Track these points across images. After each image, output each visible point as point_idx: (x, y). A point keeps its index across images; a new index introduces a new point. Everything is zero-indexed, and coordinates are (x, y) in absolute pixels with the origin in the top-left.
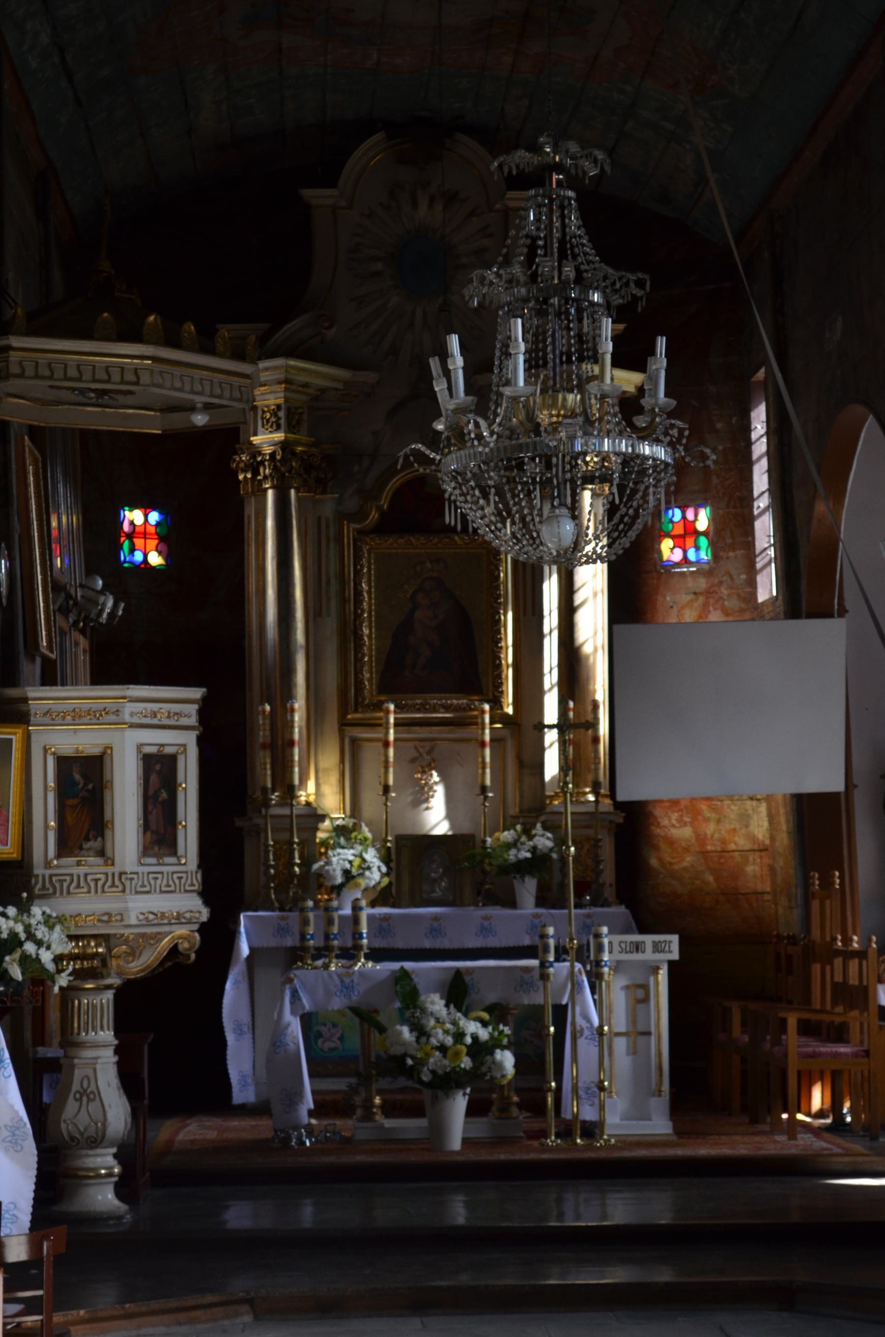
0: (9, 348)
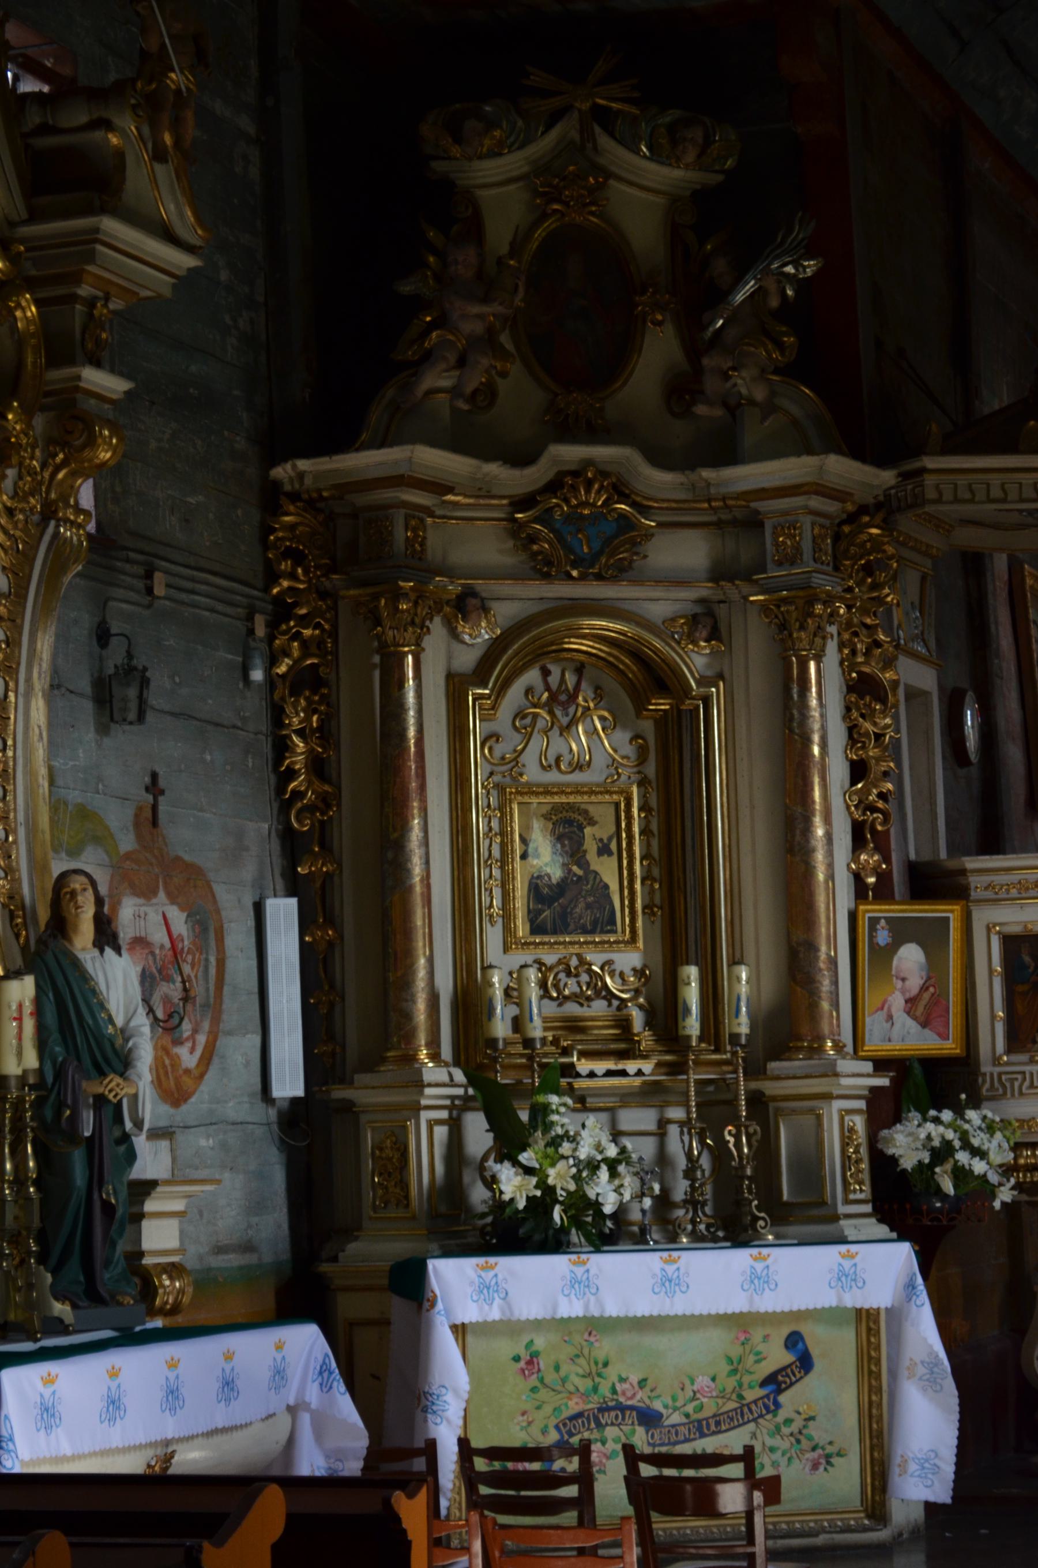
0: (924, 470)
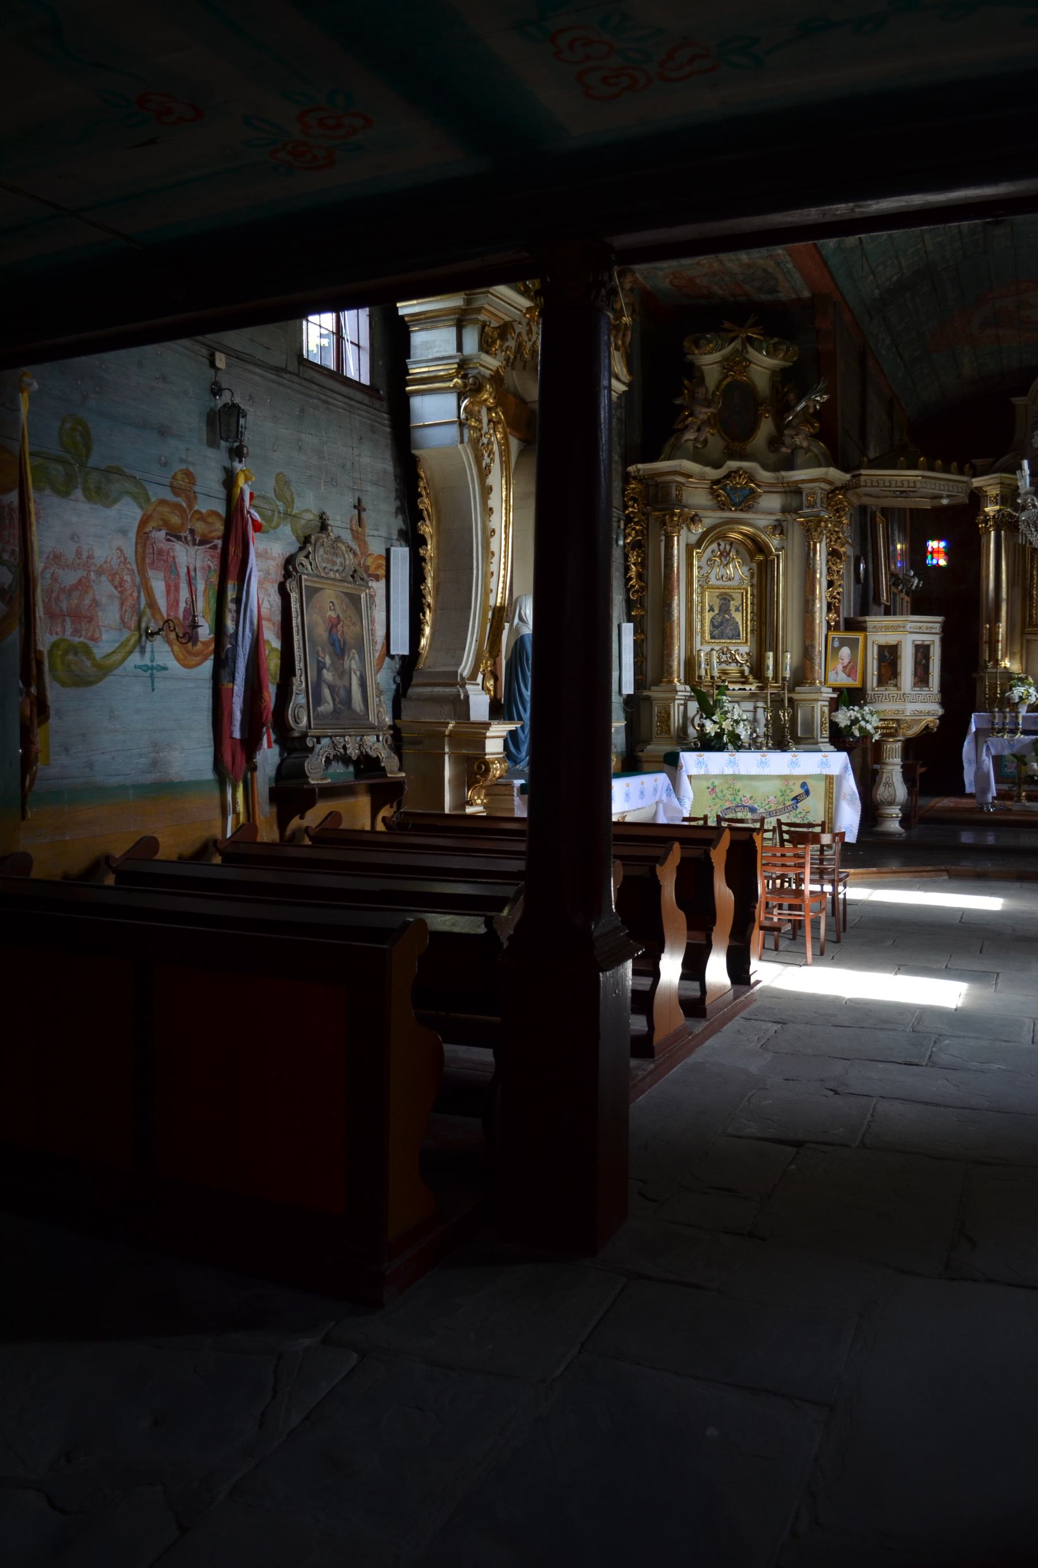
0: (860, 475)
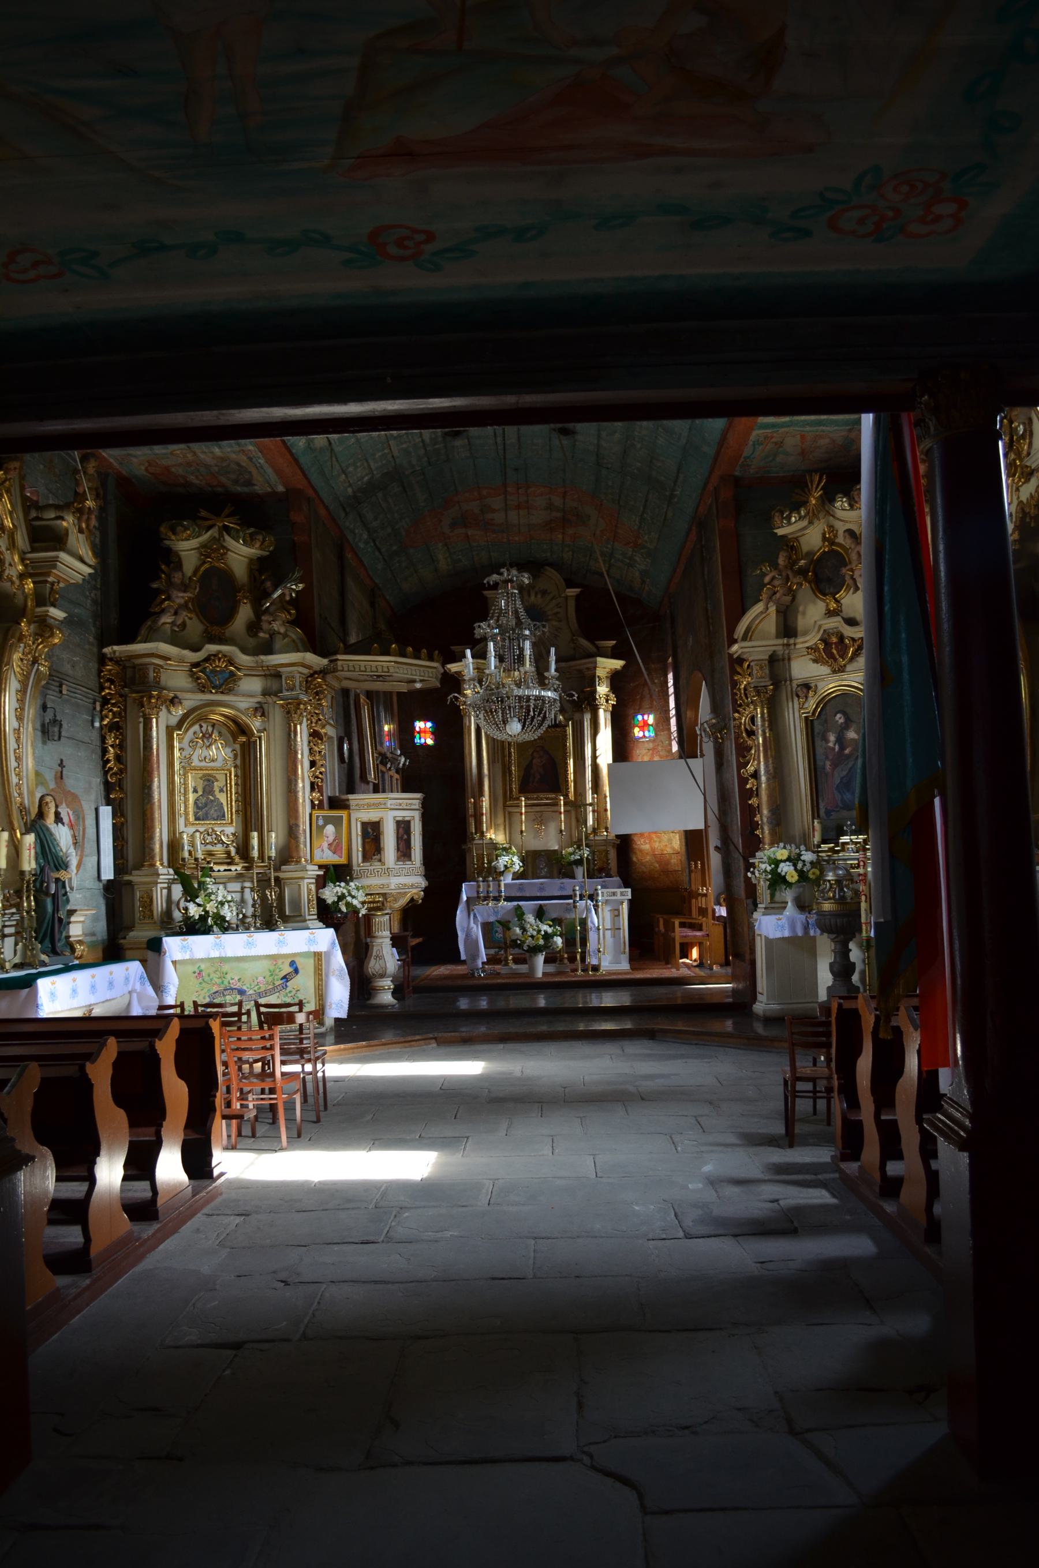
0: (337, 660)
